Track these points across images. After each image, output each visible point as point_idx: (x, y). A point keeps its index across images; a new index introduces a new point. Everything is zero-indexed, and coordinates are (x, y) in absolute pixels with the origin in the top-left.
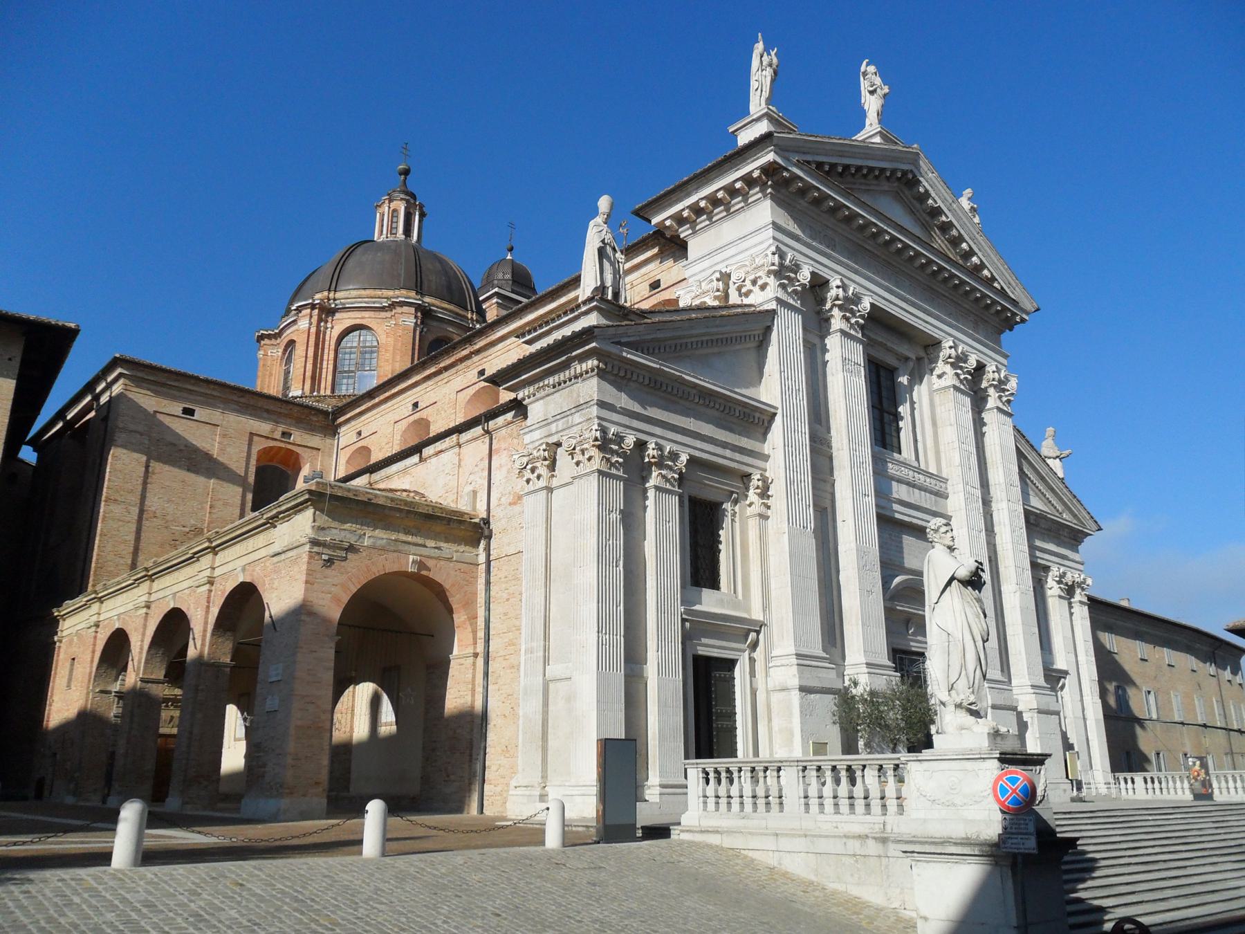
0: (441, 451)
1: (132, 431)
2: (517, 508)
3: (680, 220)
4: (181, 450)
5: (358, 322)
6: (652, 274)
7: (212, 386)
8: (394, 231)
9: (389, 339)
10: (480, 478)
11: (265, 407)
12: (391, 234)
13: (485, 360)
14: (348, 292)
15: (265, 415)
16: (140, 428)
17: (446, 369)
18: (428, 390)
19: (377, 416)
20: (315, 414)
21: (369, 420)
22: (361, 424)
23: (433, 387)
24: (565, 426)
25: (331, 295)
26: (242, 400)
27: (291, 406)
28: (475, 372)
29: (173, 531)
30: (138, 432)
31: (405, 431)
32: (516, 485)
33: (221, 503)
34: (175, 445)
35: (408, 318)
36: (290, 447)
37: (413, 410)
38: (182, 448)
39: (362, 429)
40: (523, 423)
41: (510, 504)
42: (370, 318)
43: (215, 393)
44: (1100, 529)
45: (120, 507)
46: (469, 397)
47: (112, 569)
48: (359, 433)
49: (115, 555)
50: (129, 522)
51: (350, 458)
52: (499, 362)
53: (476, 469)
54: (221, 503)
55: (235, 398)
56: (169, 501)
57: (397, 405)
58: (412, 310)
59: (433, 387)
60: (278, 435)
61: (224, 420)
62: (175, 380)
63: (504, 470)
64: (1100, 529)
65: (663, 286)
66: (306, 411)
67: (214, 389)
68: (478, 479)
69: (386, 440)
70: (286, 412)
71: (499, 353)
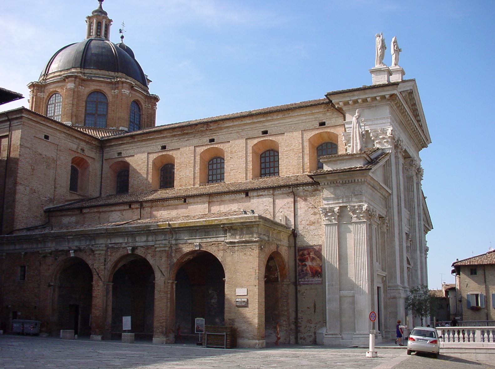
0: (260, 195)
1: (26, 147)
2: (312, 227)
3: (346, 104)
4: (44, 158)
5: (98, 88)
6: (320, 119)
7: (58, 124)
8: (99, 34)
9: (114, 99)
10: (287, 211)
11: (76, 136)
12: (97, 35)
13: (214, 134)
14: (91, 70)
15: (75, 140)
16: (29, 146)
17: (187, 134)
18: (173, 141)
19: (134, 147)
20: (95, 141)
21: (128, 148)
22: (121, 149)
23: (177, 141)
24: (347, 201)
25: (83, 71)
26: (68, 132)
27: (86, 136)
28: (208, 139)
29: (42, 200)
30: (28, 148)
31: (155, 159)
32: (311, 218)
33: (59, 185)
34: (41, 154)
35: (126, 90)
36: (83, 157)
37: (162, 149)
38: (44, 156)
39: (122, 152)
40: (314, 193)
41: (308, 225)
42: (104, 86)
43: (58, 128)
44: (433, 229)
45: (23, 187)
46: (203, 150)
47: (21, 219)
48: (120, 154)
49: (22, 212)
50: (26, 195)
51: (111, 166)
52: (224, 137)
53: (285, 207)
54: (59, 185)
55: (65, 131)
56: (40, 184)
57: (150, 145)
58: (128, 86)
59: (177, 141)
60: (79, 151)
61: (59, 142)
62: (44, 121)
63: (303, 210)
64: (433, 229)
65: (326, 125)
66: (92, 139)
67: (58, 126)
68: (286, 211)
69: (142, 161)
70: (84, 139)
71: (224, 133)
